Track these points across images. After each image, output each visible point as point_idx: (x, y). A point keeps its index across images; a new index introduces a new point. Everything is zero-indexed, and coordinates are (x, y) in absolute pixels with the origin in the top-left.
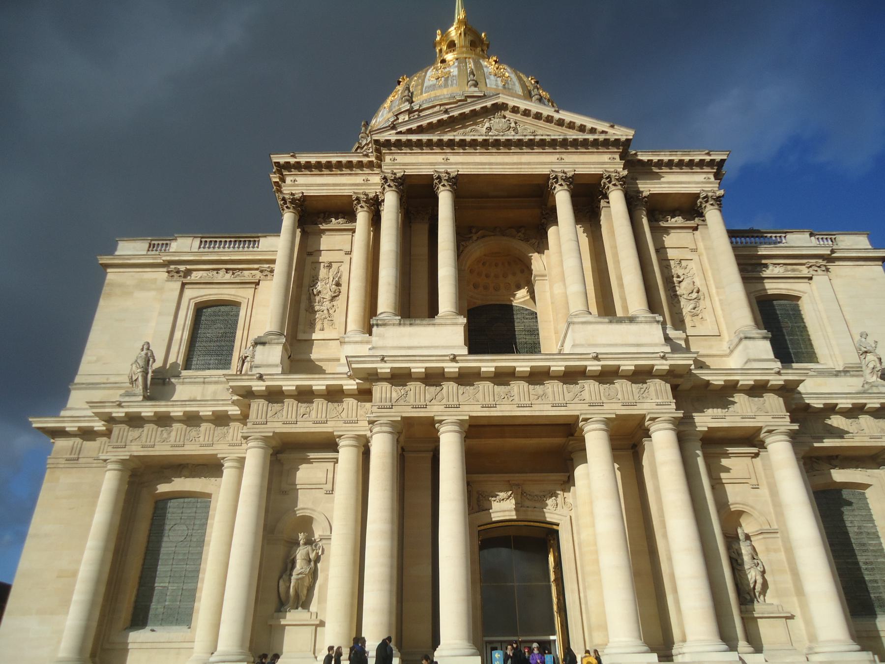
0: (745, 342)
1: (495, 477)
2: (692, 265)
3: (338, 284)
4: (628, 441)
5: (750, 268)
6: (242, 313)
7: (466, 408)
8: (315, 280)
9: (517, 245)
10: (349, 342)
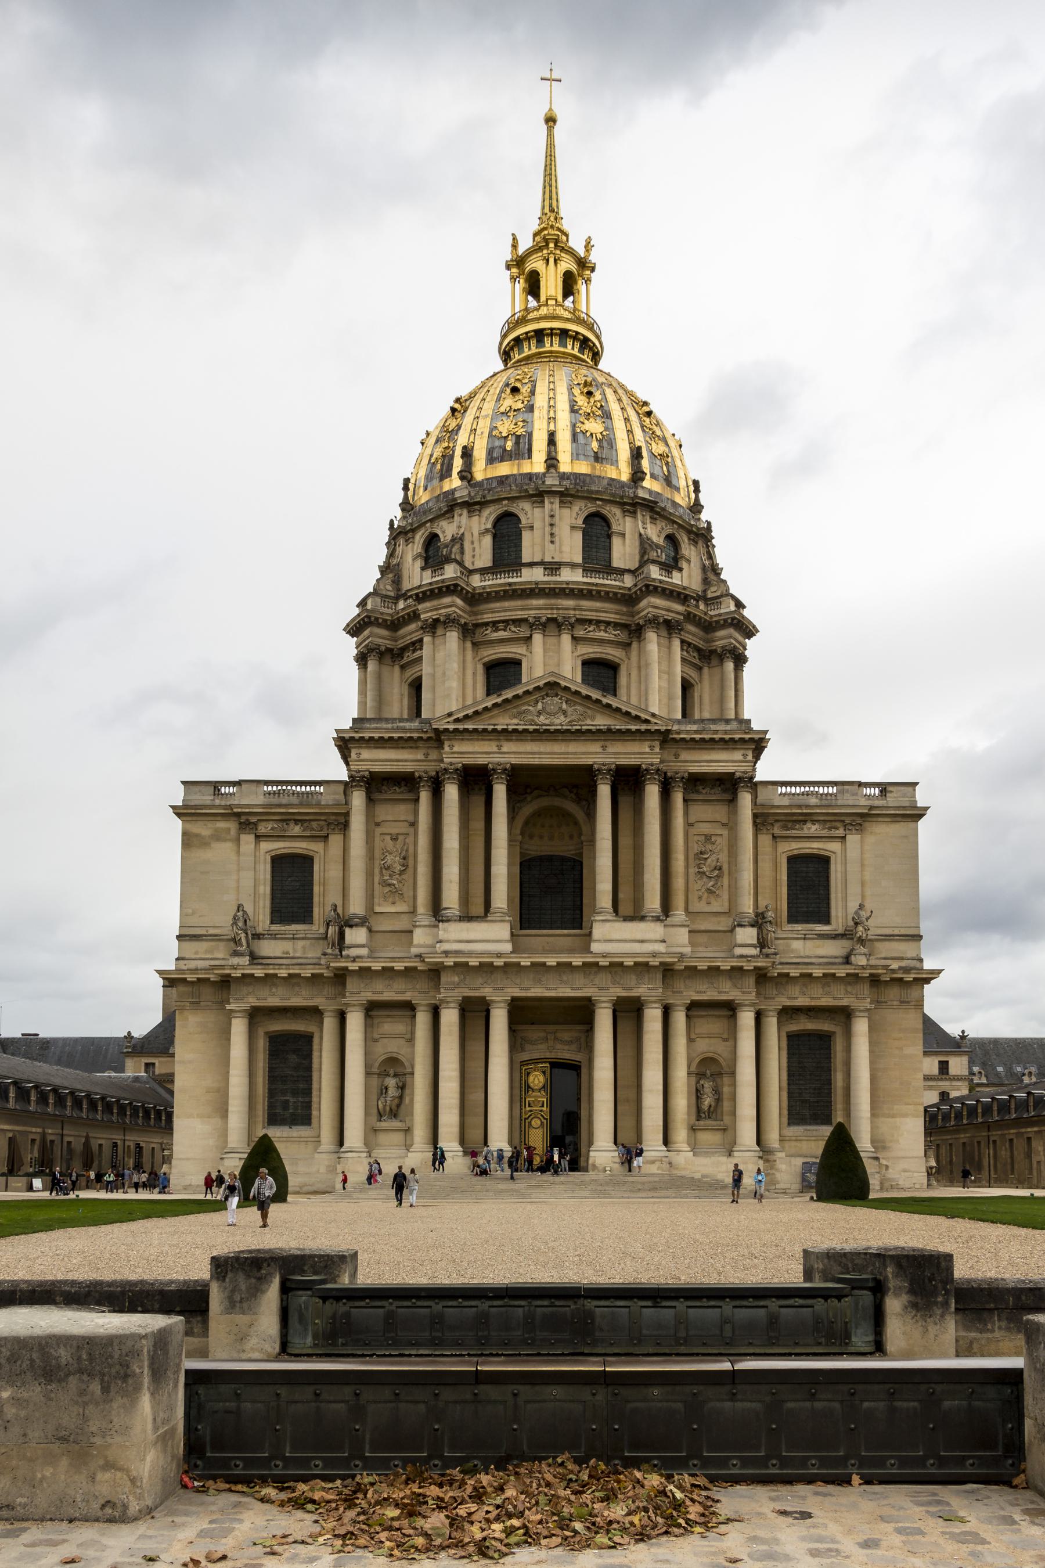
0: (738, 929)
1: (534, 1027)
2: (719, 840)
4: (629, 1012)
5: (790, 825)
6: (316, 868)
7: (509, 990)
8: (385, 852)
9: (571, 807)
10: (420, 926)
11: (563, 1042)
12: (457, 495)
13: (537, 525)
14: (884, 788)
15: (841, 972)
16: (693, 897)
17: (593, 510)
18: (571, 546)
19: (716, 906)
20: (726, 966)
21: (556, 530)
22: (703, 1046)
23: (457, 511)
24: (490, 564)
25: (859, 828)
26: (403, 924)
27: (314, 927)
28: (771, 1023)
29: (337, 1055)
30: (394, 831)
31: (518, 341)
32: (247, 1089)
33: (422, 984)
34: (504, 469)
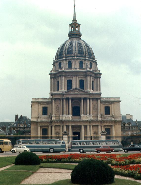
3: (59, 108)
9: (79, 101)
13: (74, 63)
16: (93, 112)
18: (78, 65)
25: (113, 103)
28: (103, 127)
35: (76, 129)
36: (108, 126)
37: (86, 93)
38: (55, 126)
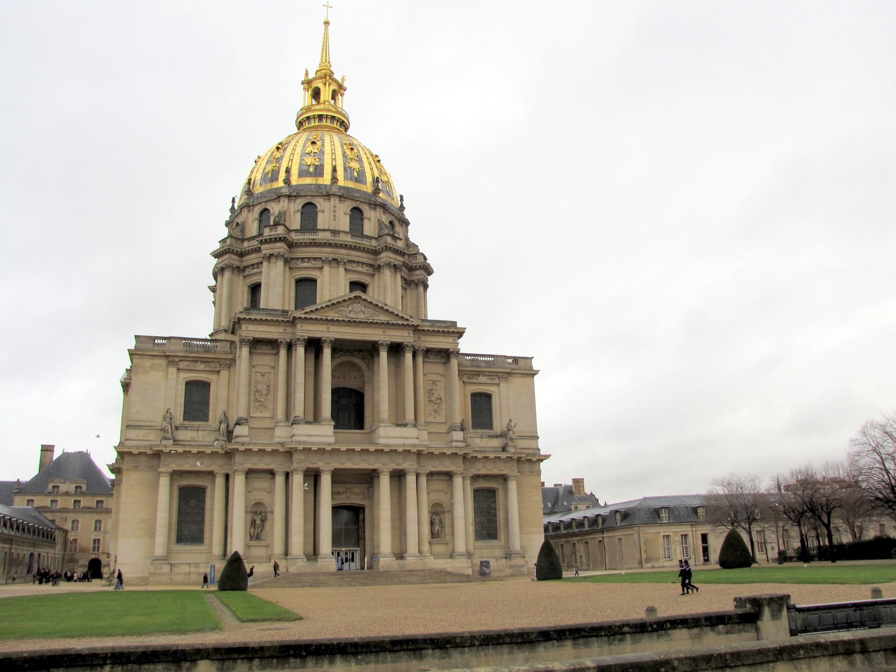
0: (454, 432)
2: (439, 383)
8: (257, 382)
9: (358, 361)
11: (356, 494)
12: (283, 191)
14: (516, 360)
15: (504, 456)
17: (355, 205)
18: (344, 223)
19: (439, 419)
20: (449, 452)
21: (337, 214)
22: (435, 497)
23: (282, 199)
24: (299, 228)
26: (267, 424)
27: (209, 423)
29: (224, 501)
30: (263, 371)
31: (308, 118)
32: (167, 521)
33: (281, 459)
34: (308, 181)
35: (346, 492)
36: (485, 477)
37: (400, 322)
38: (249, 473)
